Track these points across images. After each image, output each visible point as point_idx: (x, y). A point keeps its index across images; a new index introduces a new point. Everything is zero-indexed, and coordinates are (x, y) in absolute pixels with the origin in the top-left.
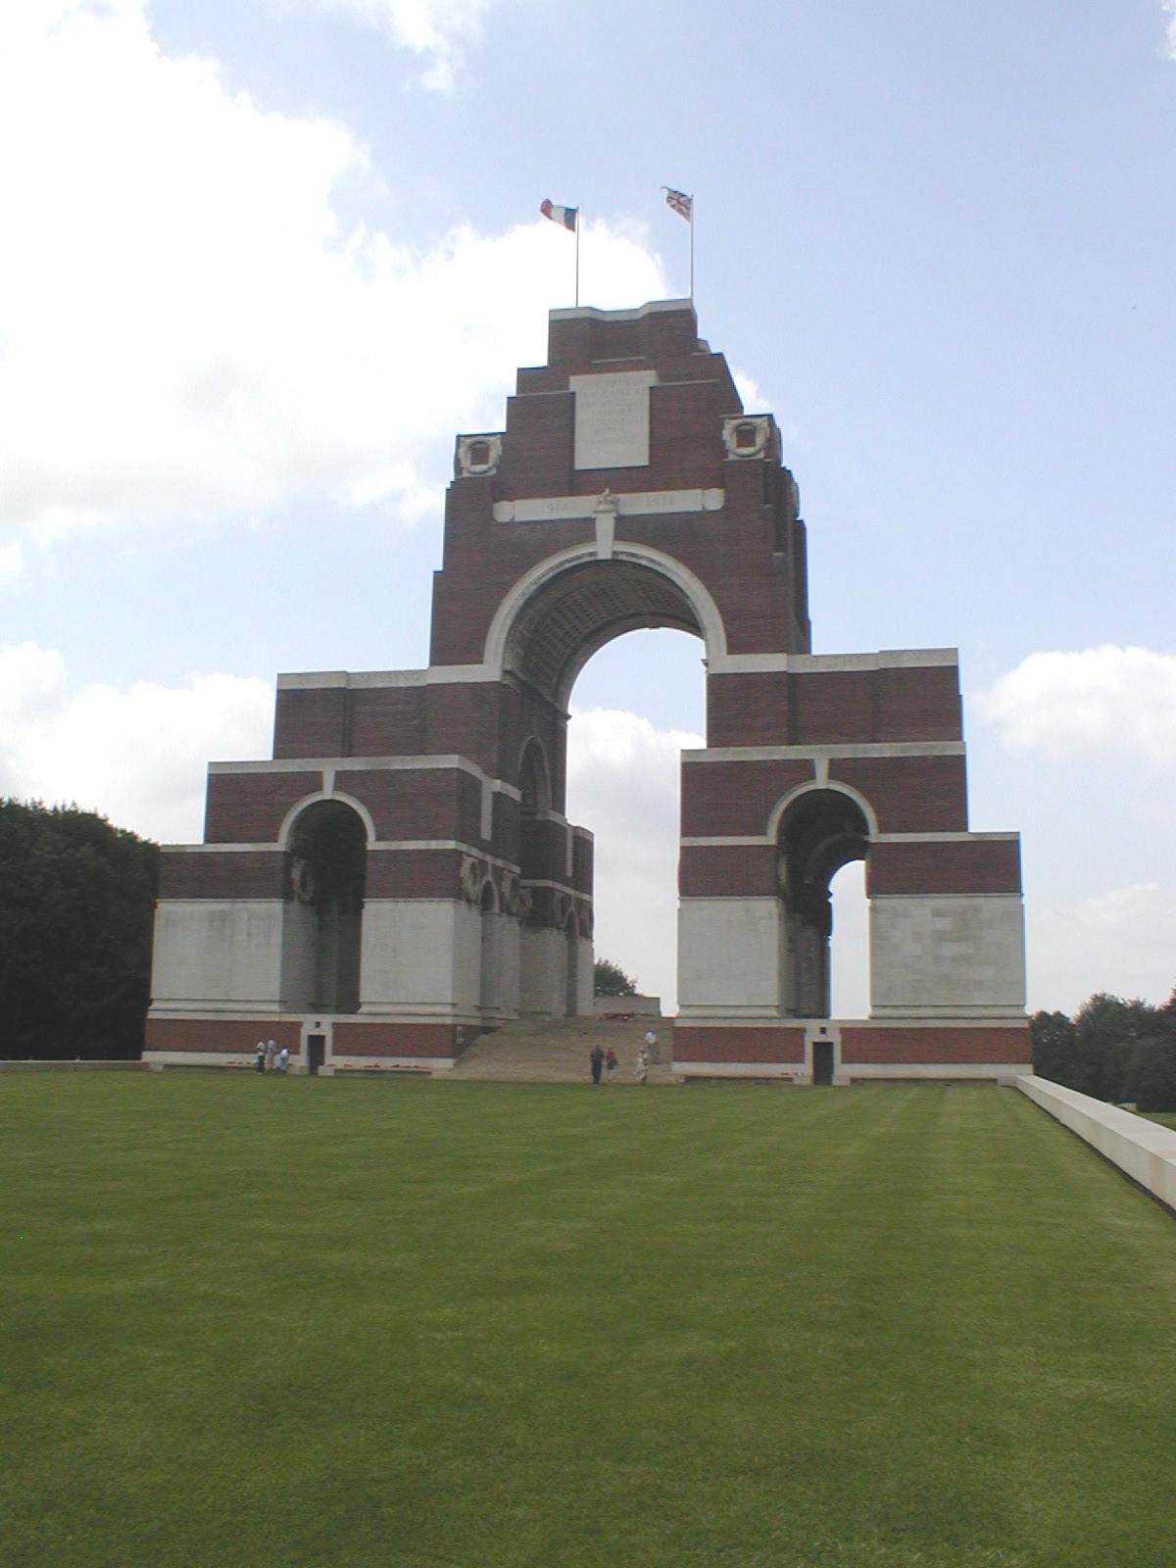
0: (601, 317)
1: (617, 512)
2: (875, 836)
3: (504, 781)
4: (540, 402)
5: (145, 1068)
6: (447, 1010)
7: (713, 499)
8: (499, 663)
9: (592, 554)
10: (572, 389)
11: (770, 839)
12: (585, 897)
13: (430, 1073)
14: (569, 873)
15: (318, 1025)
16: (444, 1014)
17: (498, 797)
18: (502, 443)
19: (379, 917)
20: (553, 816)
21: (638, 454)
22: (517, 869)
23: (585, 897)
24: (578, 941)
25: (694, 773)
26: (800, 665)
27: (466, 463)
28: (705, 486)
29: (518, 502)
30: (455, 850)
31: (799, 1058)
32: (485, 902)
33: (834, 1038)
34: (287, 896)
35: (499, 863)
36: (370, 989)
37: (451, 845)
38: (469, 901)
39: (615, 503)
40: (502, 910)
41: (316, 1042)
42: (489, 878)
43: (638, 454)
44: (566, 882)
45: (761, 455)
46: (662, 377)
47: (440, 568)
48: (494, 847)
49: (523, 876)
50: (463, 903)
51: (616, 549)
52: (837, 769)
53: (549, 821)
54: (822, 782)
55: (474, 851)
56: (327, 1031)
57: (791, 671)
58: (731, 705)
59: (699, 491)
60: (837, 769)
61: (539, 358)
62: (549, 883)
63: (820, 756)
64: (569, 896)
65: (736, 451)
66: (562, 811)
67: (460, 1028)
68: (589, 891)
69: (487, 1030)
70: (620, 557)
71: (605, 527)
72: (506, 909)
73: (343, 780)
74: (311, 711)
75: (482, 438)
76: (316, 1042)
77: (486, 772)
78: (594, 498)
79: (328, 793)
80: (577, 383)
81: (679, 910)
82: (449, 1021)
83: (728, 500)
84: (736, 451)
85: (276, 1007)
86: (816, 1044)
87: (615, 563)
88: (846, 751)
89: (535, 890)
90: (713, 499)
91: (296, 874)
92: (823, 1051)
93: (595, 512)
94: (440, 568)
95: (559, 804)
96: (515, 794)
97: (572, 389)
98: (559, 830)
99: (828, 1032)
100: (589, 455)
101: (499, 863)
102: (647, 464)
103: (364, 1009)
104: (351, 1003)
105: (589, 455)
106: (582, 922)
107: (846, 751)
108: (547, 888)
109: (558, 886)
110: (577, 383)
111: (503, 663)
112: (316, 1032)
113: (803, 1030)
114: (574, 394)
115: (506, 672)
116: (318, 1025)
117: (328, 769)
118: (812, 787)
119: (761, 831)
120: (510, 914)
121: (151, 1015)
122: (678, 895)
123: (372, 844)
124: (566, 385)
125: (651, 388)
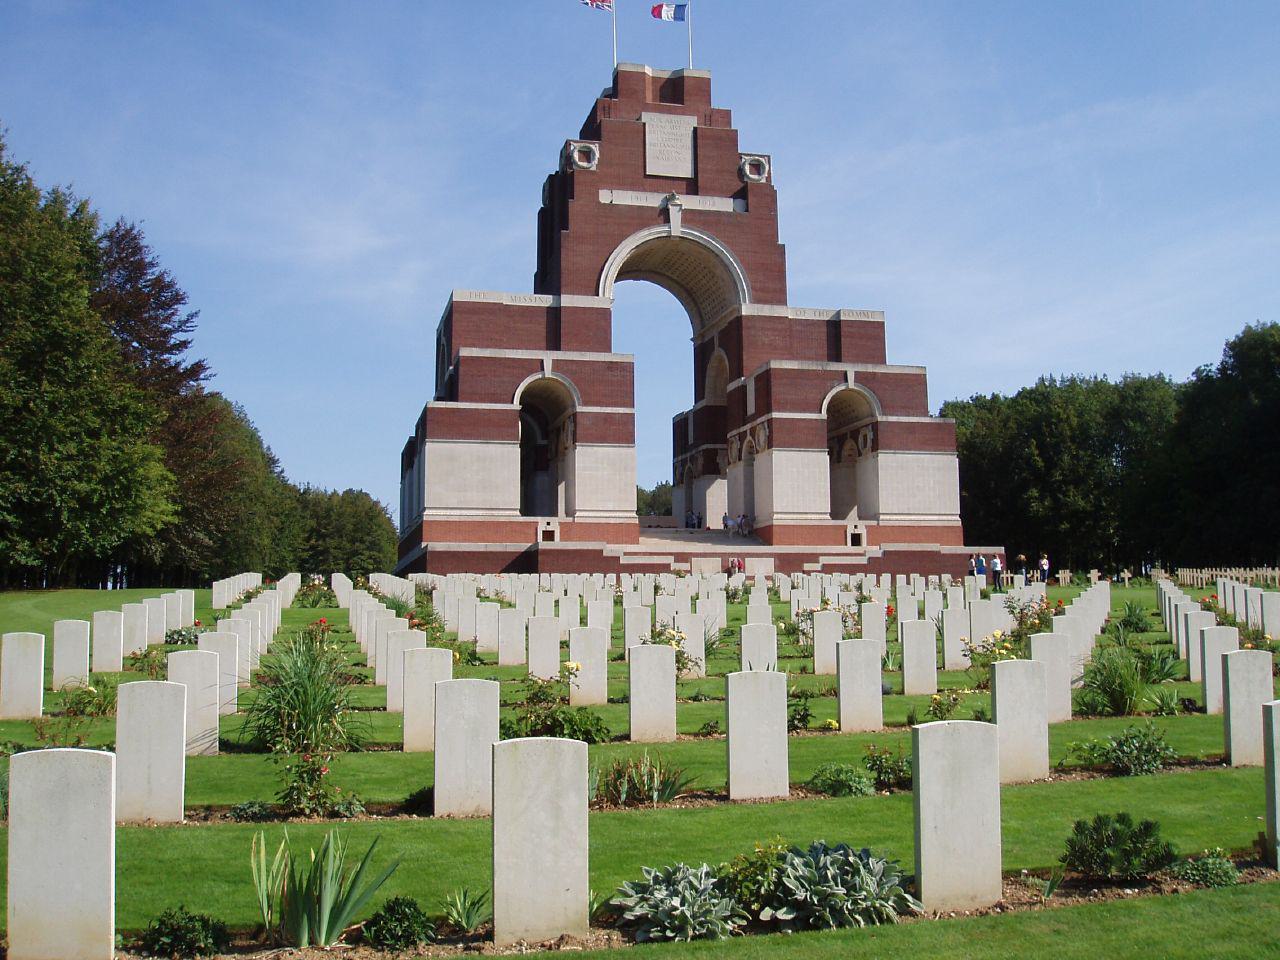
11: (824, 415)
15: (548, 524)
27: (576, 156)
33: (862, 531)
43: (686, 172)
45: (764, 181)
52: (859, 377)
73: (557, 364)
80: (646, 117)
88: (861, 368)
103: (578, 514)
107: (861, 368)
110: (646, 117)
112: (549, 528)
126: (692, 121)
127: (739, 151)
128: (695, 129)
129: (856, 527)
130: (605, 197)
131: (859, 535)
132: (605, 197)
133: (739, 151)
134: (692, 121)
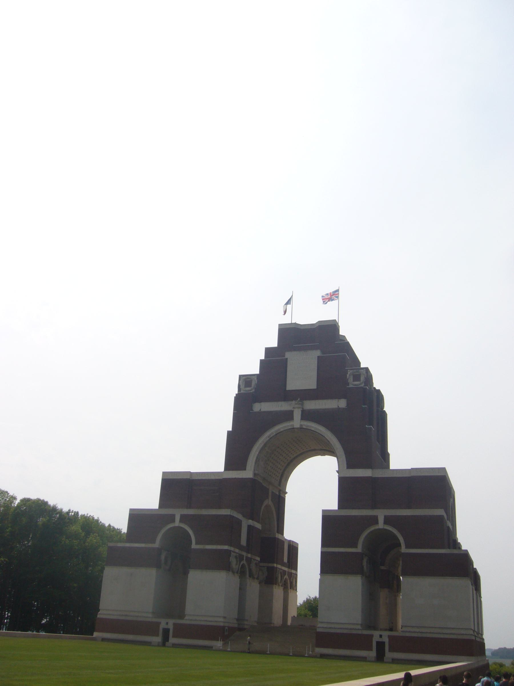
0: (299, 327)
1: (303, 408)
2: (404, 549)
3: (253, 520)
4: (274, 362)
5: (95, 639)
6: (222, 619)
7: (342, 403)
10: (286, 357)
12: (293, 571)
13: (212, 647)
14: (286, 560)
15: (167, 623)
16: (220, 622)
17: (249, 527)
18: (257, 379)
19: (195, 577)
20: (278, 536)
21: (311, 384)
22: (258, 559)
23: (293, 571)
24: (289, 591)
25: (329, 520)
26: (379, 473)
28: (339, 398)
29: (263, 404)
30: (227, 550)
31: (370, 649)
32: (242, 573)
33: (386, 640)
34: (158, 566)
35: (249, 555)
36: (190, 609)
37: (226, 547)
38: (233, 572)
39: (302, 404)
40: (250, 576)
41: (166, 632)
42: (244, 562)
43: (311, 384)
44: (283, 564)
45: (362, 385)
46: (323, 352)
47: (231, 429)
48: (248, 549)
49: (261, 561)
50: (231, 573)
53: (276, 538)
54: (381, 525)
55: (237, 550)
56: (171, 627)
57: (374, 476)
58: (347, 489)
59: (337, 400)
60: (388, 520)
61: (274, 343)
62: (275, 565)
63: (381, 514)
64: (286, 571)
65: (352, 384)
66: (282, 534)
67: (226, 628)
68: (296, 569)
69: (241, 629)
70: (304, 427)
71: (297, 414)
72: (251, 575)
74: (176, 487)
75: (249, 377)
76: (166, 632)
77: (244, 516)
78: (294, 402)
79: (177, 523)
80: (288, 355)
81: (320, 580)
82: (222, 624)
83: (348, 404)
84: (352, 384)
85: (150, 615)
86: (378, 643)
87: (301, 428)
89: (268, 568)
90: (342, 403)
91: (163, 557)
92: (380, 645)
93: (294, 408)
94: (231, 429)
95: (281, 530)
96: (258, 526)
97: (286, 357)
98: (282, 542)
99: (383, 637)
100: (293, 384)
101: (249, 555)
102: (316, 388)
103: (186, 618)
104: (182, 616)
105: (292, 385)
106: (291, 583)
108: (274, 567)
109: (279, 566)
110: (288, 355)
111: (254, 470)
112: (166, 627)
113: (372, 636)
115: (255, 474)
116: (167, 623)
117: (178, 513)
118: (376, 527)
119: (355, 546)
120: (254, 578)
121: (98, 616)
122: (319, 573)
123: (194, 546)
125: (318, 357)
126: (318, 353)
128: (318, 357)
129: (381, 636)
131: (383, 643)
132: (258, 407)
134: (318, 353)
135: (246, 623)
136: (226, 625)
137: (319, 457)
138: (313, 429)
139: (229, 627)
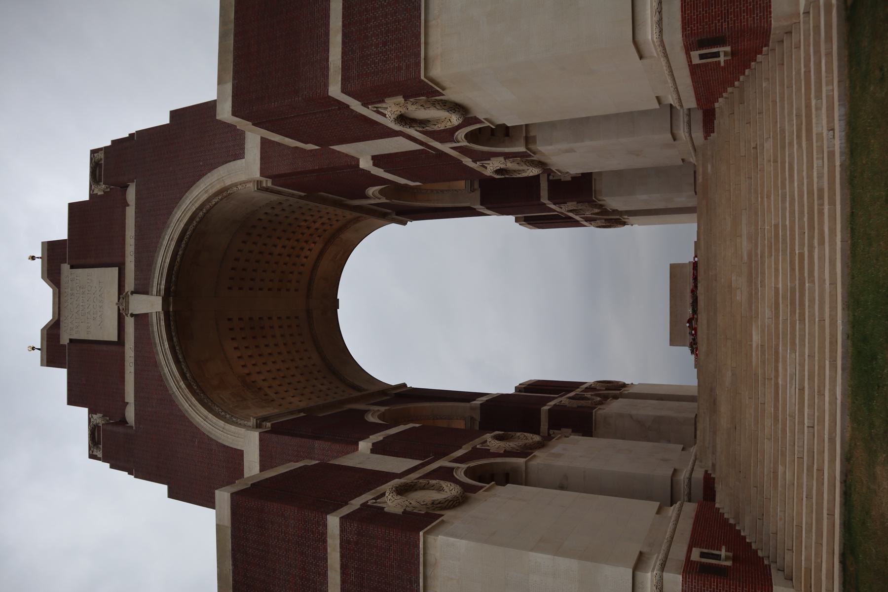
8: (242, 431)
9: (158, 319)
51: (155, 292)
90: (131, 194)
94: (164, 488)
114: (71, 340)
115: (258, 426)
124: (65, 346)
125: (72, 267)
127: (87, 198)
128: (72, 267)
130: (130, 414)
132: (130, 414)
133: (87, 198)
135: (683, 476)
136: (679, 551)
137: (340, 312)
138: (168, 261)
139: (693, 543)
